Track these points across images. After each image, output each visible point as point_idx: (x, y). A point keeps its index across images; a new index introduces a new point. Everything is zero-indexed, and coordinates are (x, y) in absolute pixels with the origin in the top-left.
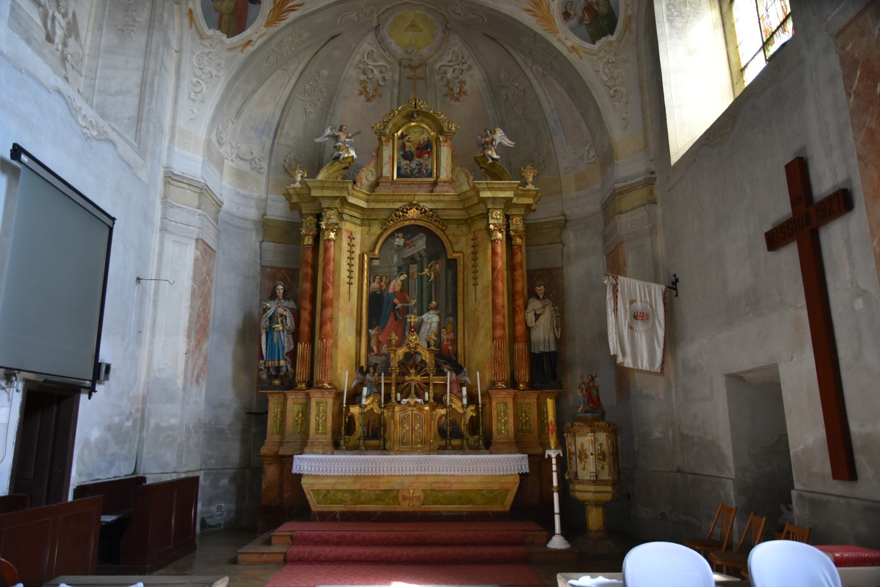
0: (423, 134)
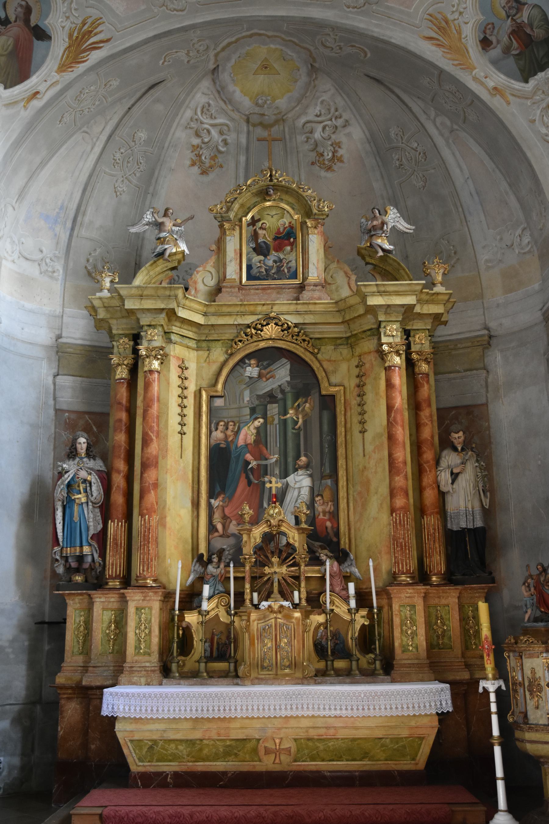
0: (283, 218)
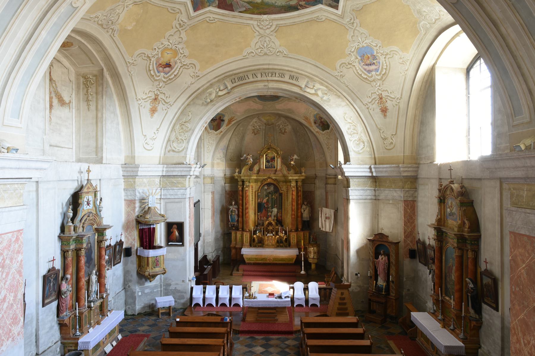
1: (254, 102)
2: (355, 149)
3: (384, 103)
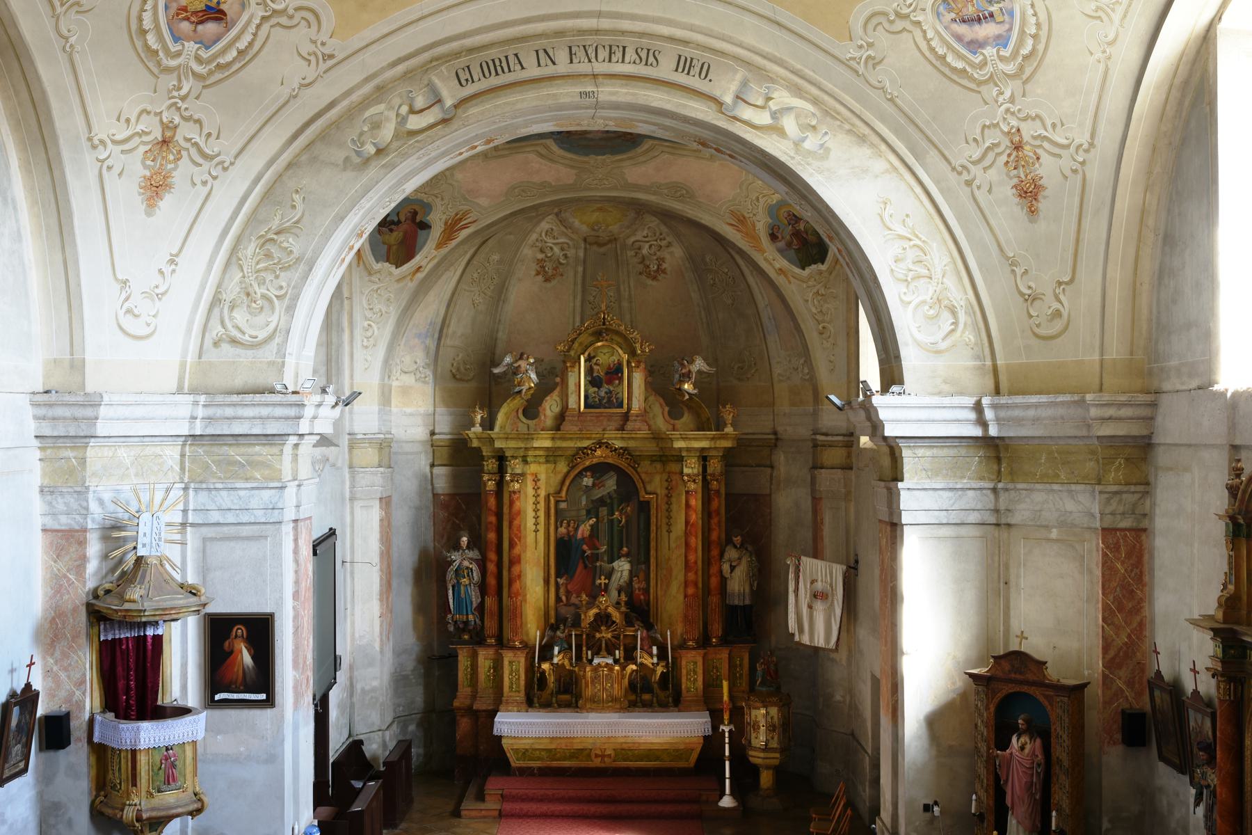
0: (613, 355)
1: (541, 156)
2: (920, 337)
3: (1026, 161)
